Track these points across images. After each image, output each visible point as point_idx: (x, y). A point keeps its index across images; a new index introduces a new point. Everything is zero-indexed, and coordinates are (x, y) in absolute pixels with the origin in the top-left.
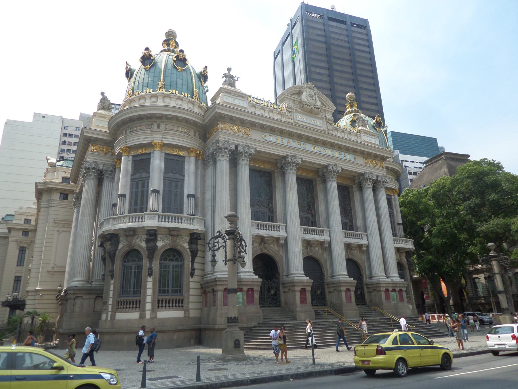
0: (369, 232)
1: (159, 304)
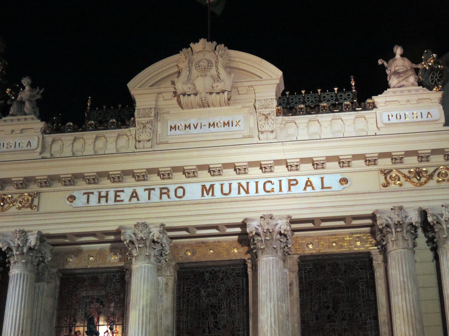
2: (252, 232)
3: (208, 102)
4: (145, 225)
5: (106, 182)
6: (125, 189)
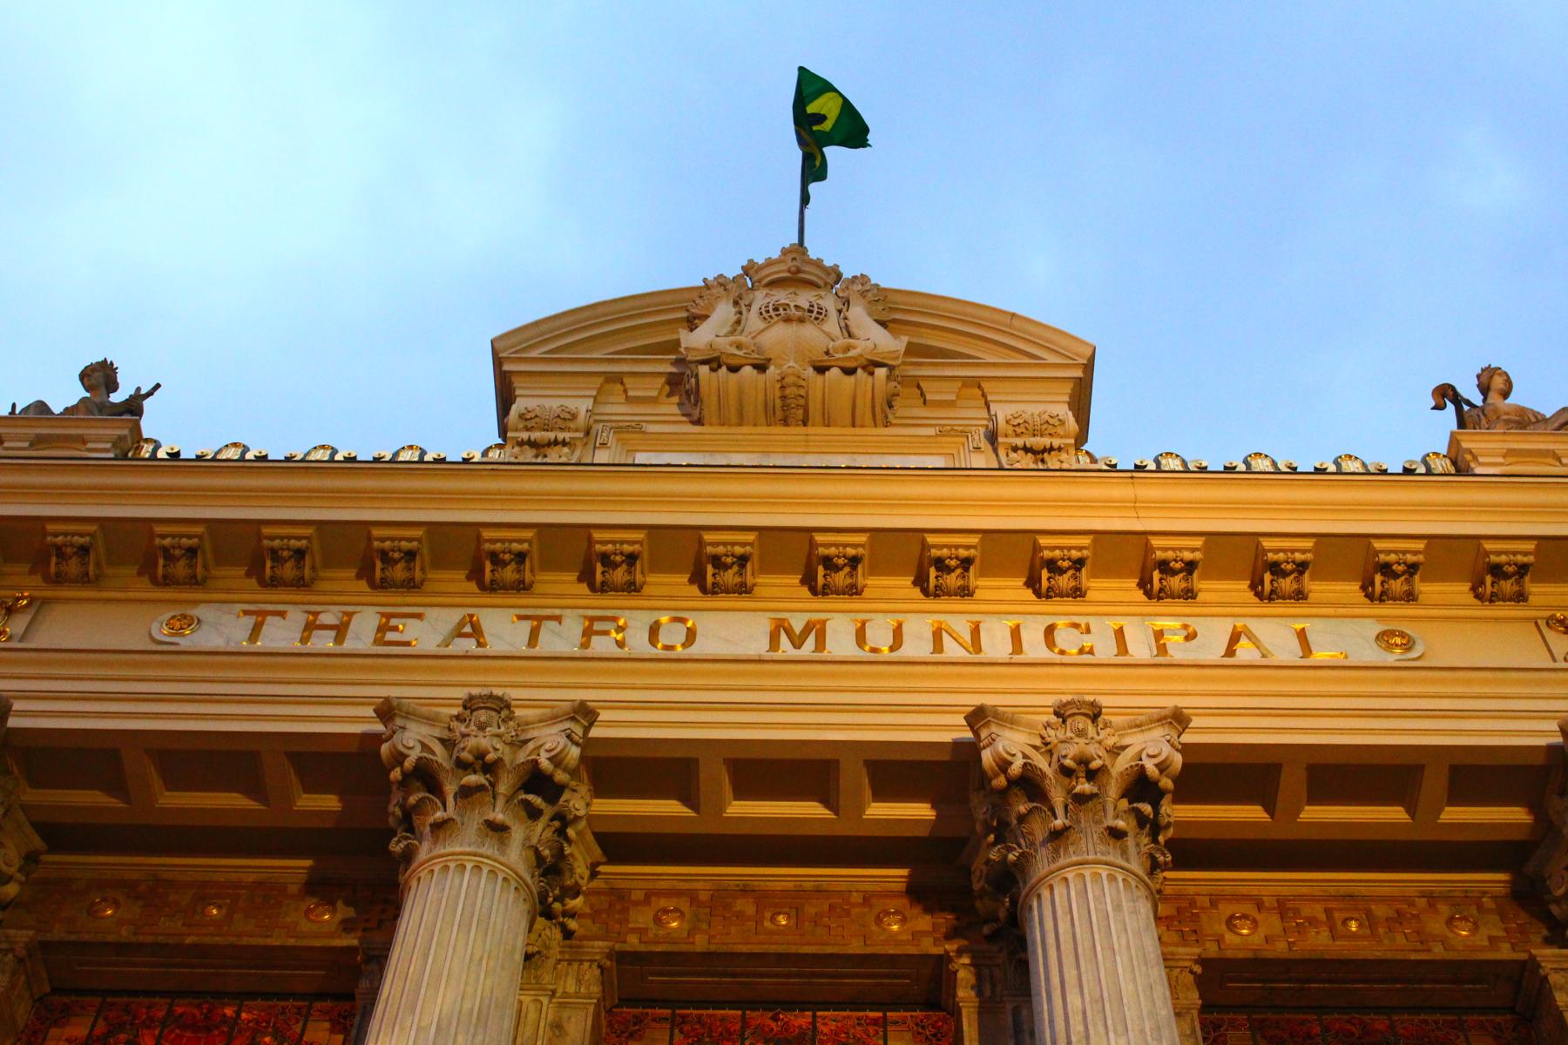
2: (1004, 765)
3: (805, 397)
4: (501, 706)
6: (431, 613)
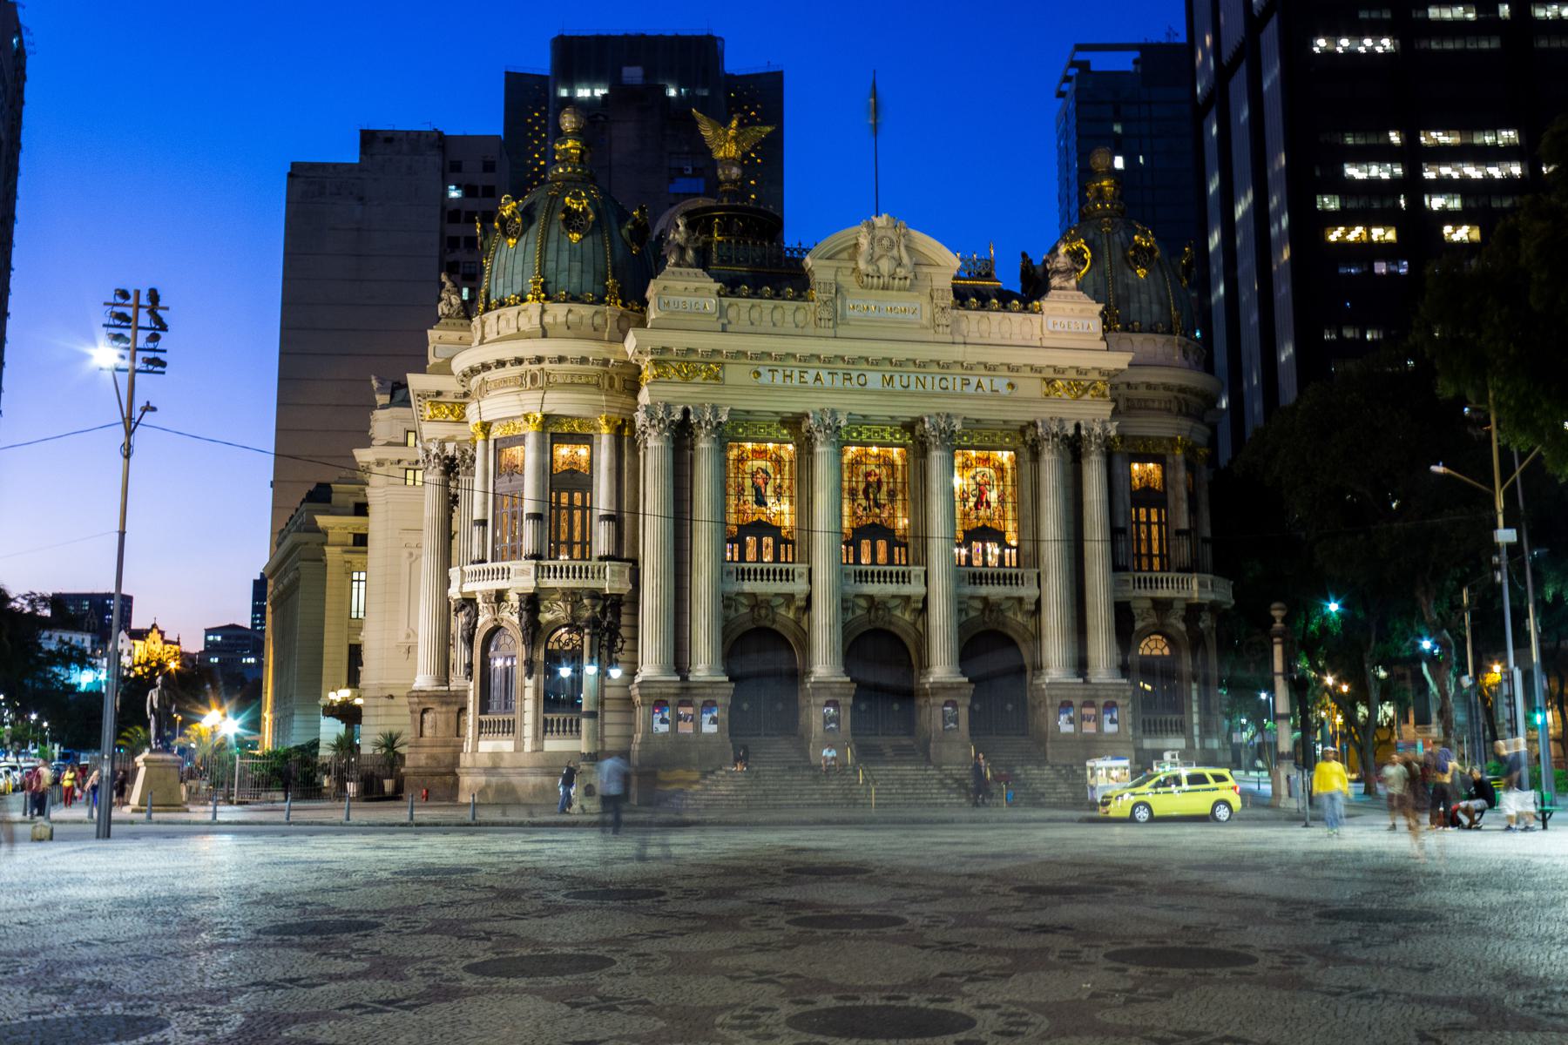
0: (1042, 567)
1: (545, 728)
5: (792, 362)
